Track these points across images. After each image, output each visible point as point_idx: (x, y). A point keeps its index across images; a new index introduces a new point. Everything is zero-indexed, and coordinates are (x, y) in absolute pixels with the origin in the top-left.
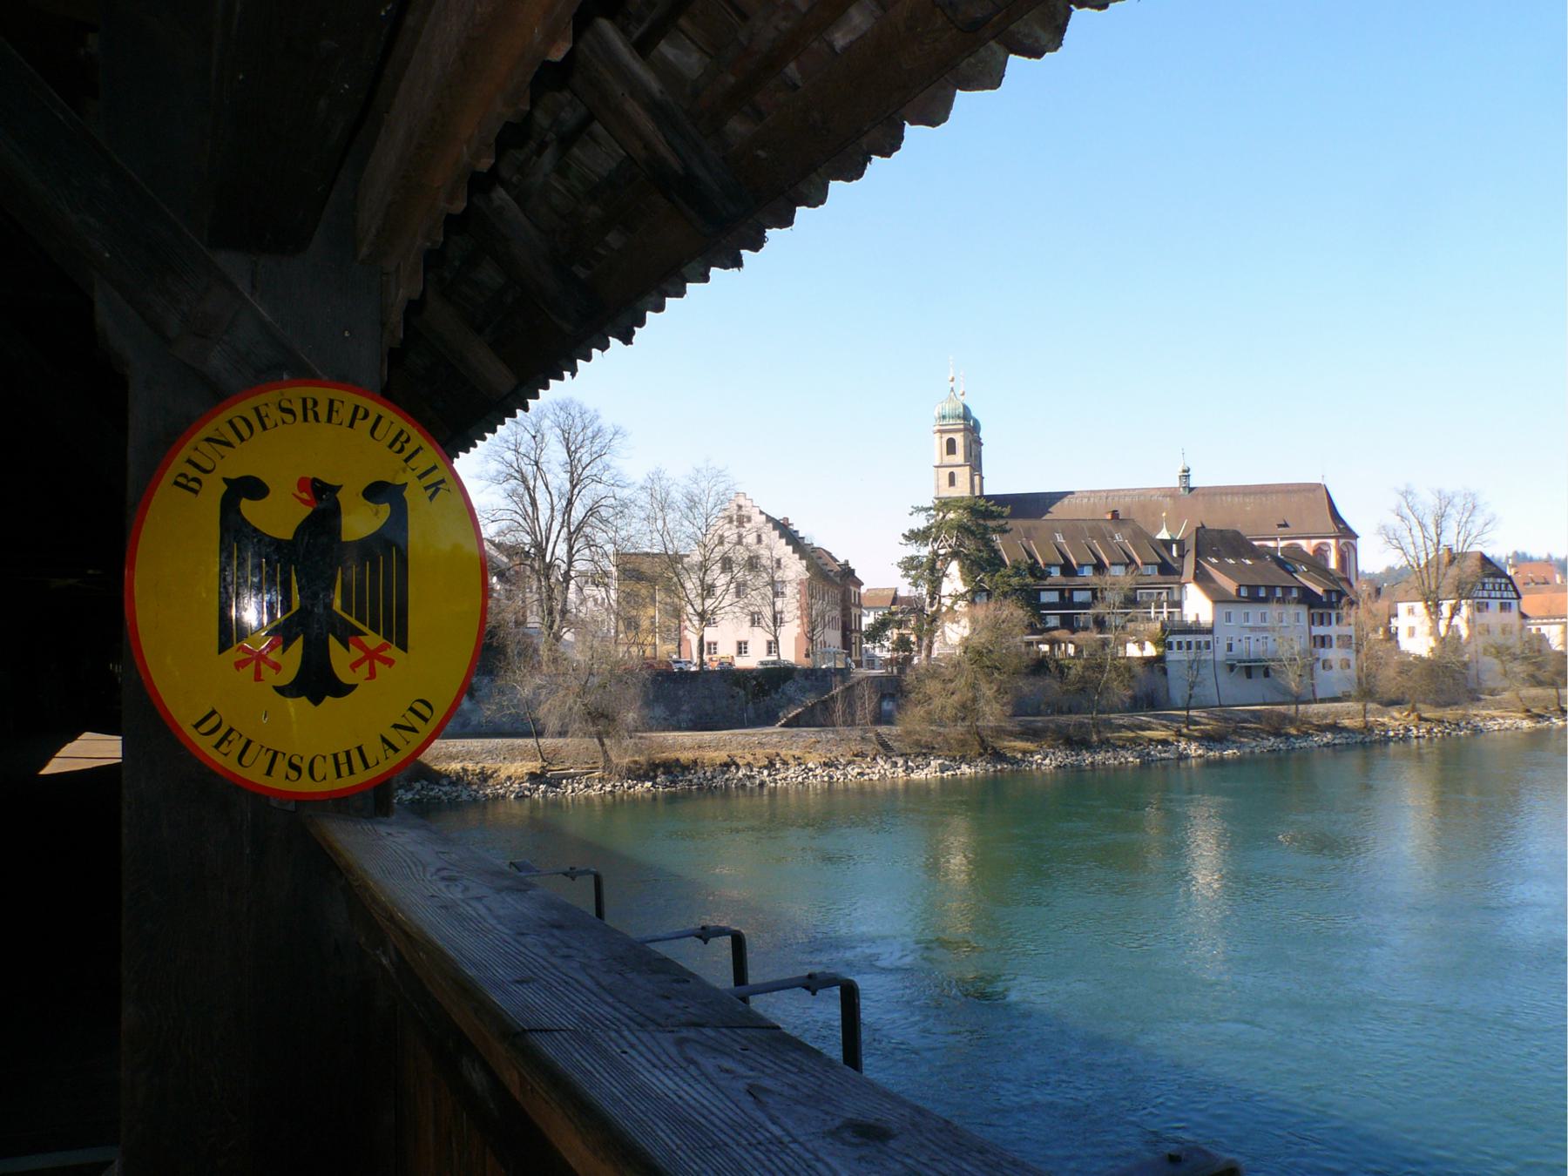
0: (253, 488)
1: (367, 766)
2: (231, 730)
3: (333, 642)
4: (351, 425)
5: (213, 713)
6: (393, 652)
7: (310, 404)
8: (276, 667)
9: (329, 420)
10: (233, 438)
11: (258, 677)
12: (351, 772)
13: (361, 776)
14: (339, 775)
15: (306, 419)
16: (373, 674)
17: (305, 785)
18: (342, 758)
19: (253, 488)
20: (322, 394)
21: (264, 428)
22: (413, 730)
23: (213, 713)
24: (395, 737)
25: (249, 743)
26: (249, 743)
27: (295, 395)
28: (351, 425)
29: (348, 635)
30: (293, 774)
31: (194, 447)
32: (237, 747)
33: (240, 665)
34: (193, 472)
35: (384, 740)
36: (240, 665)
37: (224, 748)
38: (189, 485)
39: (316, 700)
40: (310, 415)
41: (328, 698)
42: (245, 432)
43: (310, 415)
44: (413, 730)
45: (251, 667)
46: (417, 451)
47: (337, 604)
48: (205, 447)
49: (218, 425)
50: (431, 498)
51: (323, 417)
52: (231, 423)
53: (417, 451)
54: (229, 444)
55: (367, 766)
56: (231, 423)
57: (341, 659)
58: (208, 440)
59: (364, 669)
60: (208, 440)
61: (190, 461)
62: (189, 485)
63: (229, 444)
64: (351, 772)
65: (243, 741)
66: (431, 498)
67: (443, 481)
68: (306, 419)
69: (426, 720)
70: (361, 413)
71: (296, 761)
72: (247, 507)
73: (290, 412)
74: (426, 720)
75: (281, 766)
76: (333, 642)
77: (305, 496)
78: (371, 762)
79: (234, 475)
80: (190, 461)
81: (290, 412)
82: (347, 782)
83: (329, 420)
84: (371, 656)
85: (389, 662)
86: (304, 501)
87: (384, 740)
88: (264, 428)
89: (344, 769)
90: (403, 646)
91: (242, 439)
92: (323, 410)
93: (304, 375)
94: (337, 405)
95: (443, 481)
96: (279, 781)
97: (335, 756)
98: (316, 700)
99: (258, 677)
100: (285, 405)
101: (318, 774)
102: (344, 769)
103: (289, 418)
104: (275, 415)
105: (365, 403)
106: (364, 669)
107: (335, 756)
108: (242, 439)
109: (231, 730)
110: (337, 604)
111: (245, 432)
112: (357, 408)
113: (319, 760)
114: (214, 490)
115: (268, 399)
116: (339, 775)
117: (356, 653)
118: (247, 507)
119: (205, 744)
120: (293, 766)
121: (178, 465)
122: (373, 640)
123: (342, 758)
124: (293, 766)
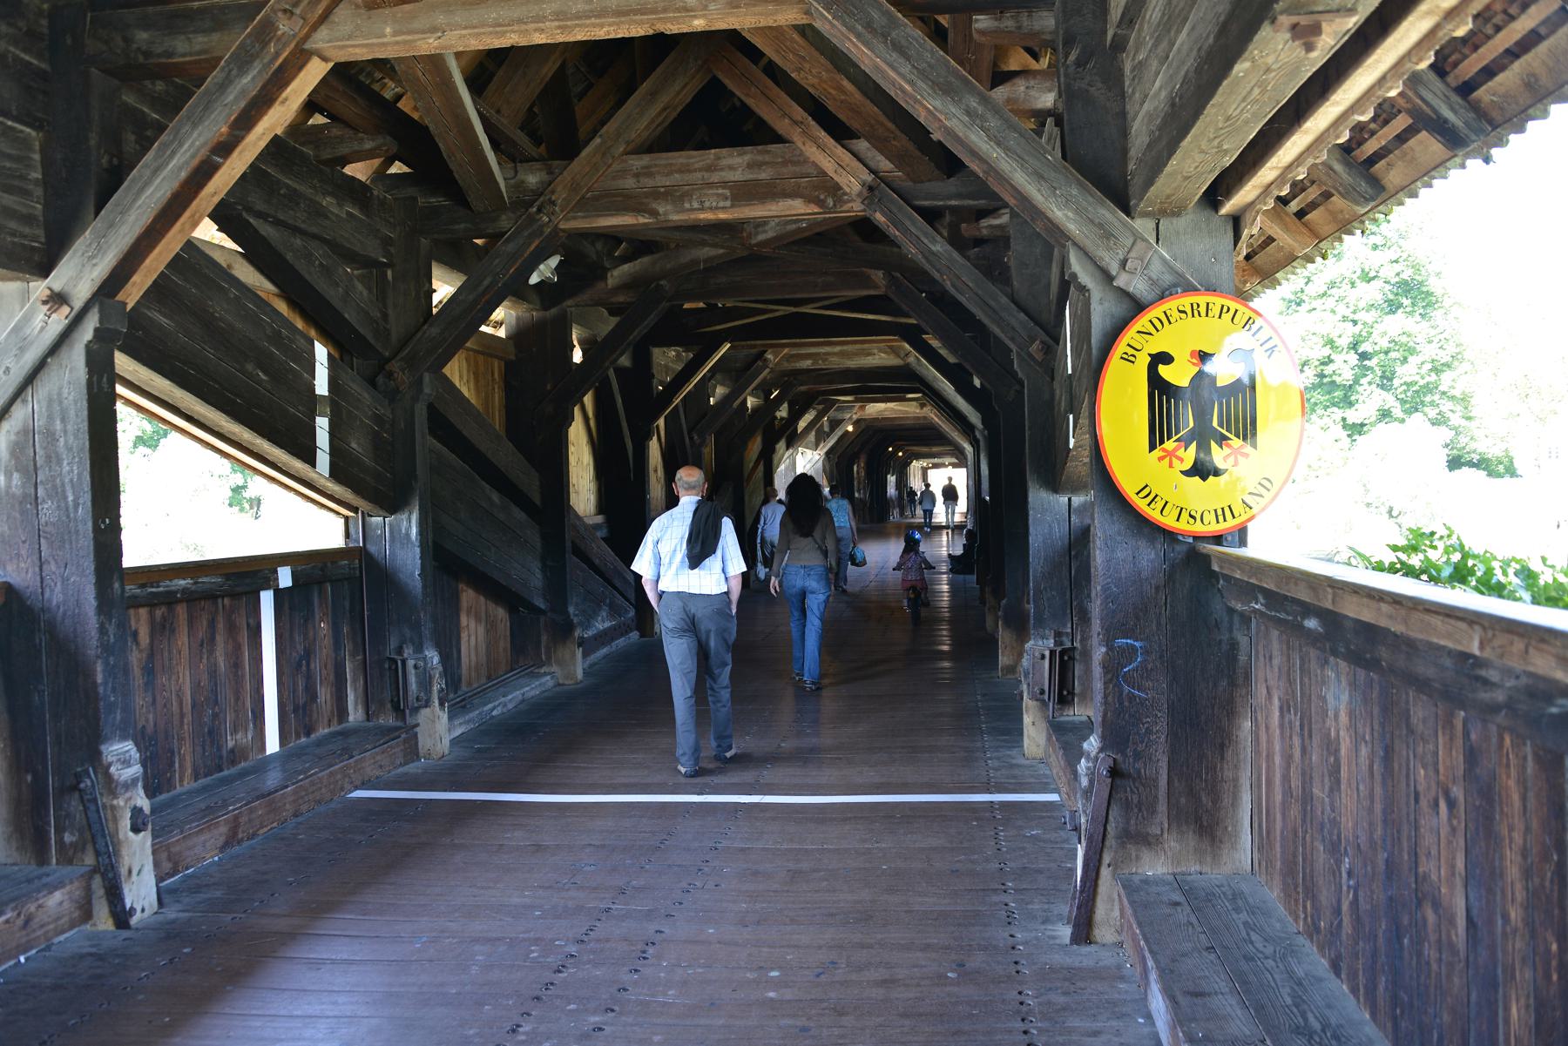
0: (1163, 358)
1: (1234, 517)
2: (1157, 496)
3: (1213, 445)
4: (1220, 317)
5: (1147, 486)
6: (1248, 449)
7: (1195, 306)
8: (1181, 460)
9: (1207, 315)
10: (1153, 330)
11: (1171, 465)
12: (1225, 520)
13: (1231, 523)
14: (1218, 522)
15: (1193, 316)
16: (1236, 464)
17: (1198, 528)
18: (1220, 512)
19: (1163, 358)
20: (1202, 300)
21: (1170, 323)
22: (1261, 496)
23: (1147, 486)
24: (1249, 500)
25: (1167, 502)
26: (1167, 502)
27: (1186, 302)
28: (1220, 317)
29: (1222, 440)
30: (1192, 521)
31: (1130, 336)
32: (1160, 505)
33: (1161, 459)
34: (1131, 351)
35: (1244, 502)
36: (1161, 459)
37: (1152, 505)
38: (1129, 359)
39: (1204, 478)
40: (1196, 313)
41: (1211, 477)
42: (1159, 325)
43: (1196, 313)
44: (1261, 496)
45: (1167, 460)
46: (1259, 330)
47: (1215, 424)
48: (1138, 336)
49: (1142, 322)
50: (1269, 357)
51: (1203, 312)
52: (1151, 321)
53: (1259, 330)
54: (1150, 334)
55: (1234, 517)
56: (1151, 321)
57: (1218, 456)
58: (1138, 332)
59: (1231, 460)
60: (1138, 332)
61: (1129, 345)
62: (1129, 359)
63: (1150, 334)
64: (1225, 520)
65: (1164, 502)
66: (1269, 357)
67: (1276, 346)
68: (1193, 316)
69: (1268, 490)
70: (1225, 309)
71: (1193, 513)
72: (1163, 370)
73: (1184, 312)
74: (1268, 490)
75: (1185, 515)
76: (1213, 445)
77: (1194, 361)
78: (1236, 514)
79: (1154, 352)
80: (1129, 345)
81: (1184, 312)
82: (1222, 526)
83: (1207, 315)
84: (1236, 452)
85: (1246, 455)
86: (1194, 364)
87: (1244, 502)
88: (1170, 323)
89: (1221, 518)
90: (1254, 446)
91: (1158, 331)
92: (1203, 310)
93: (1190, 289)
94: (1211, 306)
95: (1276, 346)
96: (1183, 525)
97: (1216, 511)
98: (1204, 478)
99: (1171, 465)
100: (1181, 308)
101: (1206, 521)
102: (1221, 518)
103: (1183, 315)
104: (1175, 315)
105: (1227, 302)
106: (1231, 460)
107: (1216, 511)
108: (1158, 331)
109: (1157, 496)
110: (1215, 424)
111: (1159, 325)
112: (1223, 306)
113: (1206, 513)
114: (1143, 361)
115: (1171, 305)
116: (1218, 522)
117: (1226, 450)
118: (1163, 370)
119: (1141, 504)
120: (1191, 516)
121: (1121, 348)
122: (1236, 442)
123: (1220, 512)
124: (1191, 516)
